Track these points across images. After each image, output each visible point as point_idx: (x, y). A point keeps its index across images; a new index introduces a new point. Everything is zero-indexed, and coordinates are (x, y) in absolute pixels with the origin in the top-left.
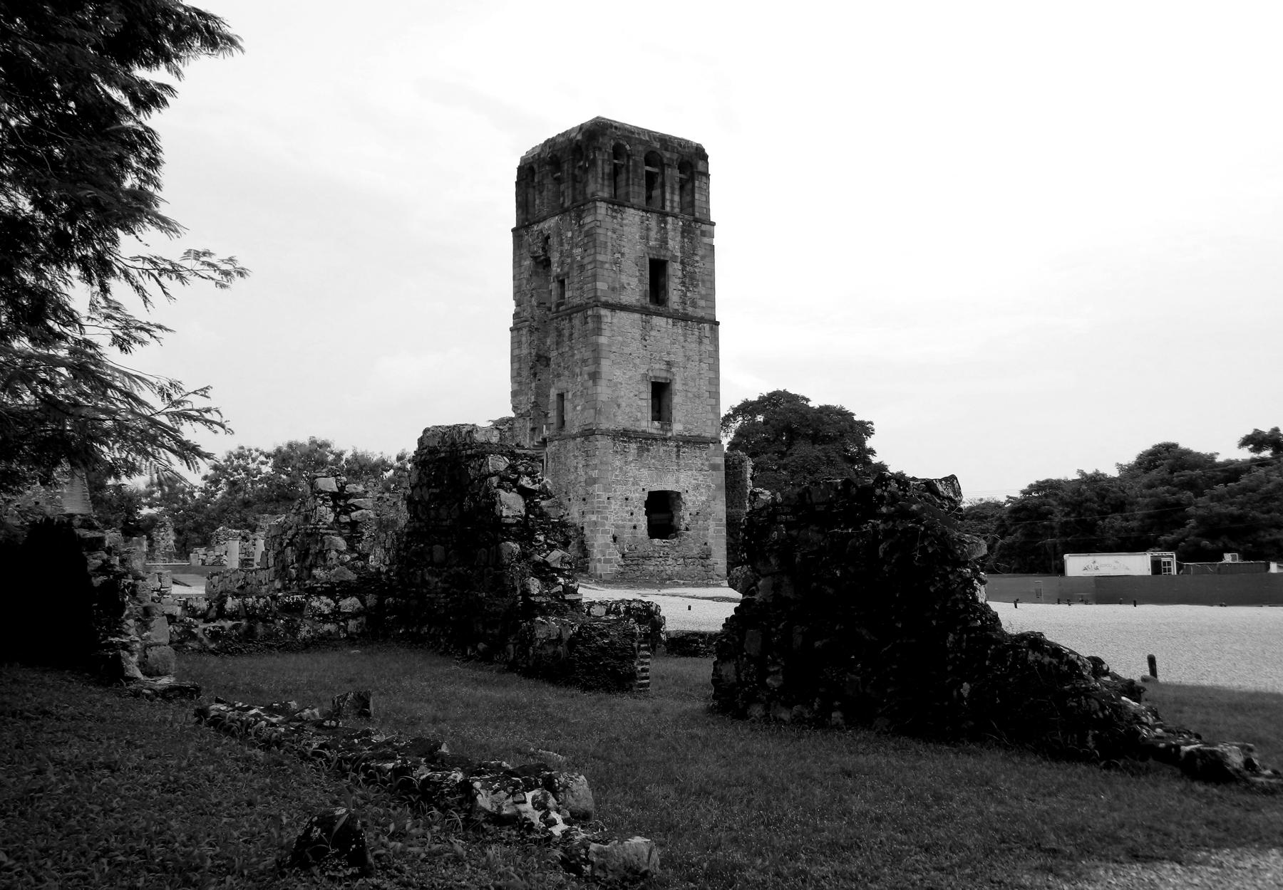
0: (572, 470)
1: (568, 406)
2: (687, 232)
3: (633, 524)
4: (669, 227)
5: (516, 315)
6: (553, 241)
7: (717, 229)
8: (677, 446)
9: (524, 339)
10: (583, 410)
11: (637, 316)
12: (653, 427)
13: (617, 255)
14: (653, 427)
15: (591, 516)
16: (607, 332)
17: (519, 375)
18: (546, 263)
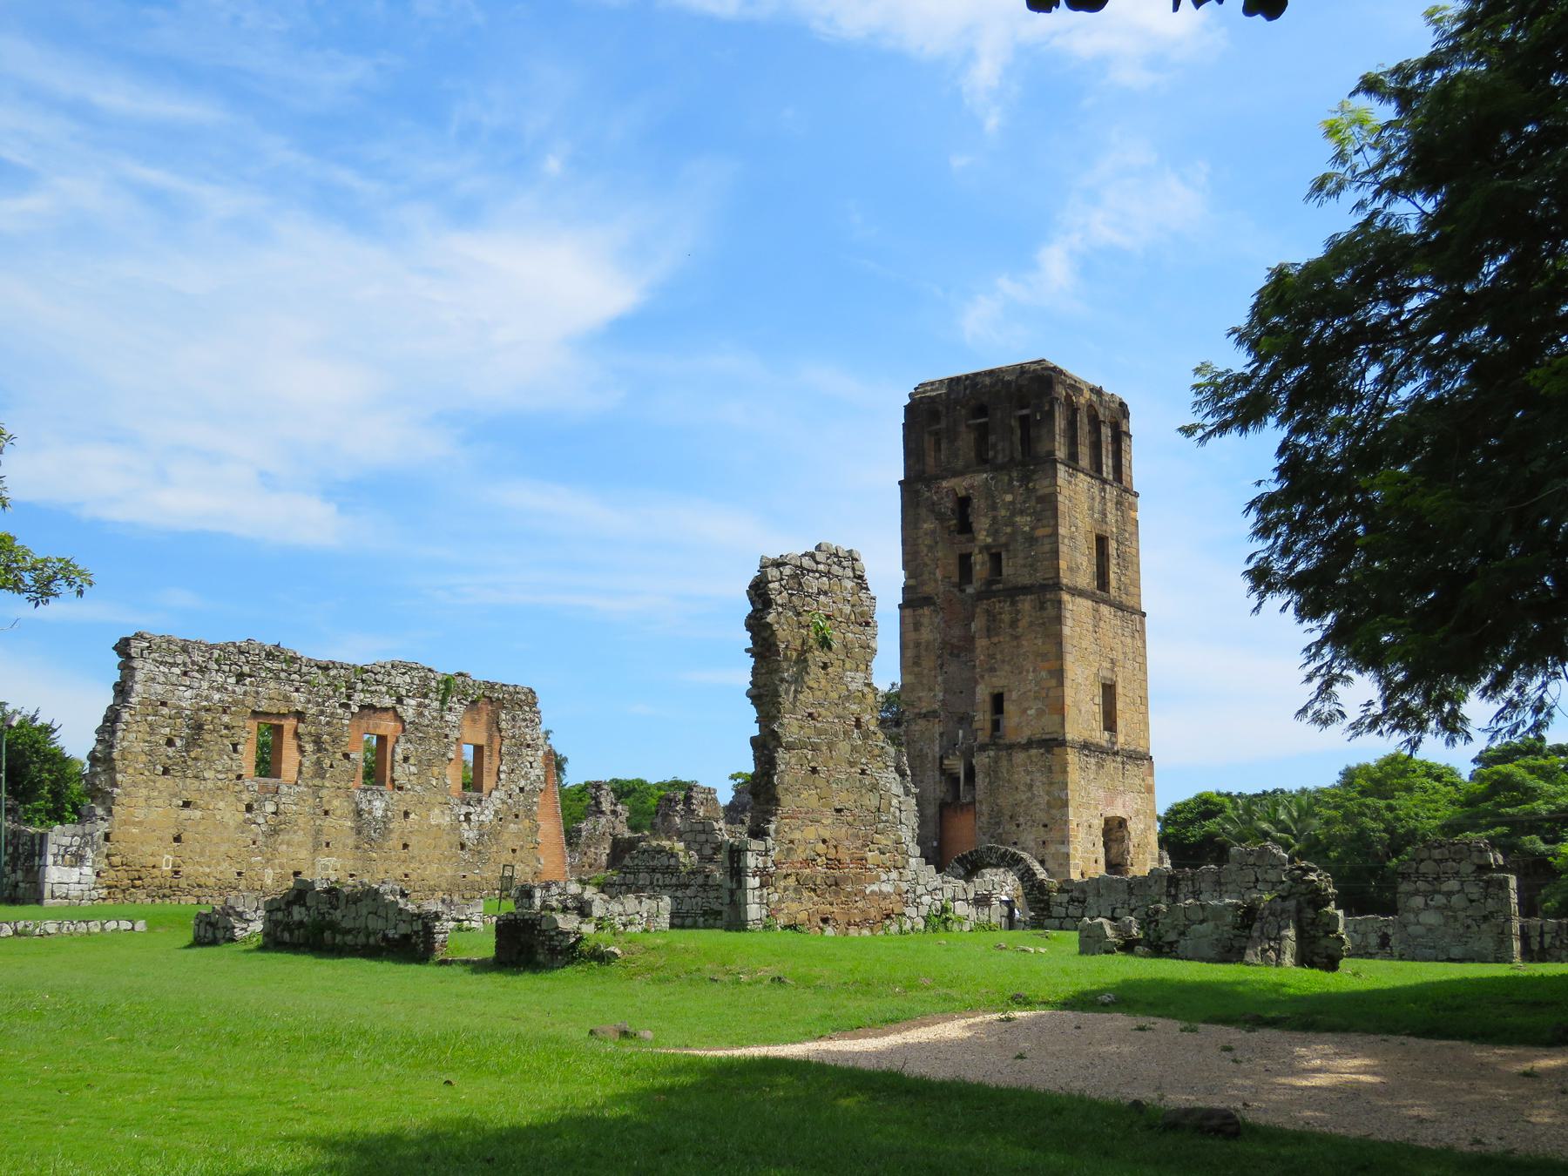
0: (1022, 788)
1: (1008, 706)
2: (1119, 504)
3: (1093, 857)
4: (1107, 496)
5: (906, 589)
6: (978, 503)
7: (1140, 502)
8: (1123, 763)
9: (925, 621)
10: (1040, 713)
11: (1089, 603)
12: (1102, 737)
13: (1073, 529)
14: (1102, 737)
15: (1059, 846)
16: (1069, 622)
17: (917, 662)
18: (965, 527)
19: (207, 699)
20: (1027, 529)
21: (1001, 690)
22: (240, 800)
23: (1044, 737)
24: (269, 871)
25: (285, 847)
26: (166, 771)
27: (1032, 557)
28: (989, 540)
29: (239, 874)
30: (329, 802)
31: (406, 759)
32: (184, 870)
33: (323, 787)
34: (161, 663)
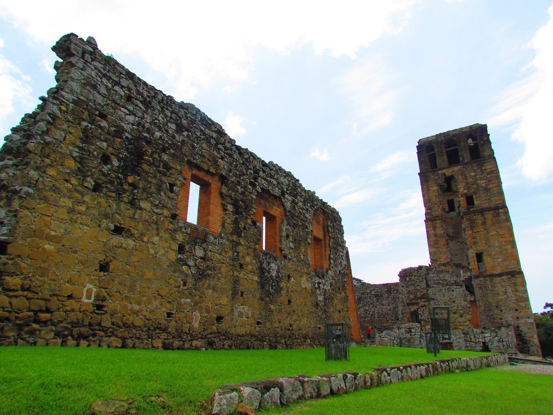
9: (438, 225)
17: (436, 242)
19: (148, 131)
20: (484, 185)
21: (482, 251)
22: (175, 239)
23: (508, 270)
24: (197, 313)
25: (211, 291)
26: (97, 188)
27: (489, 196)
28: (465, 191)
29: (169, 315)
30: (243, 257)
31: (288, 236)
32: (110, 304)
33: (239, 244)
34: (105, 76)
